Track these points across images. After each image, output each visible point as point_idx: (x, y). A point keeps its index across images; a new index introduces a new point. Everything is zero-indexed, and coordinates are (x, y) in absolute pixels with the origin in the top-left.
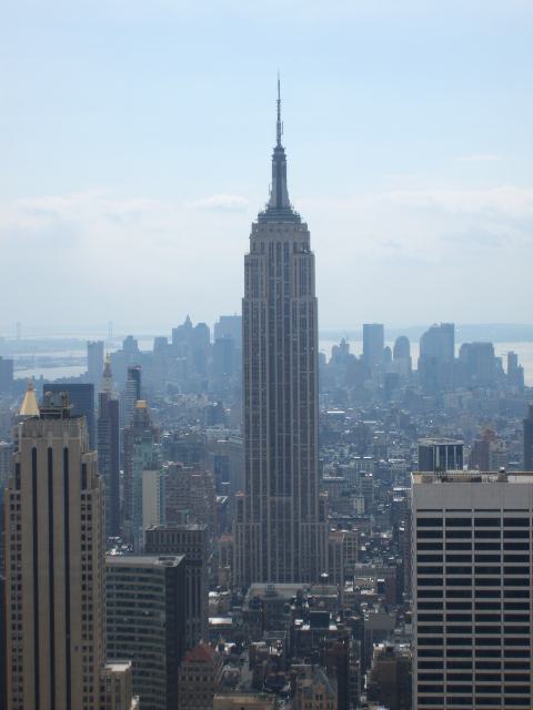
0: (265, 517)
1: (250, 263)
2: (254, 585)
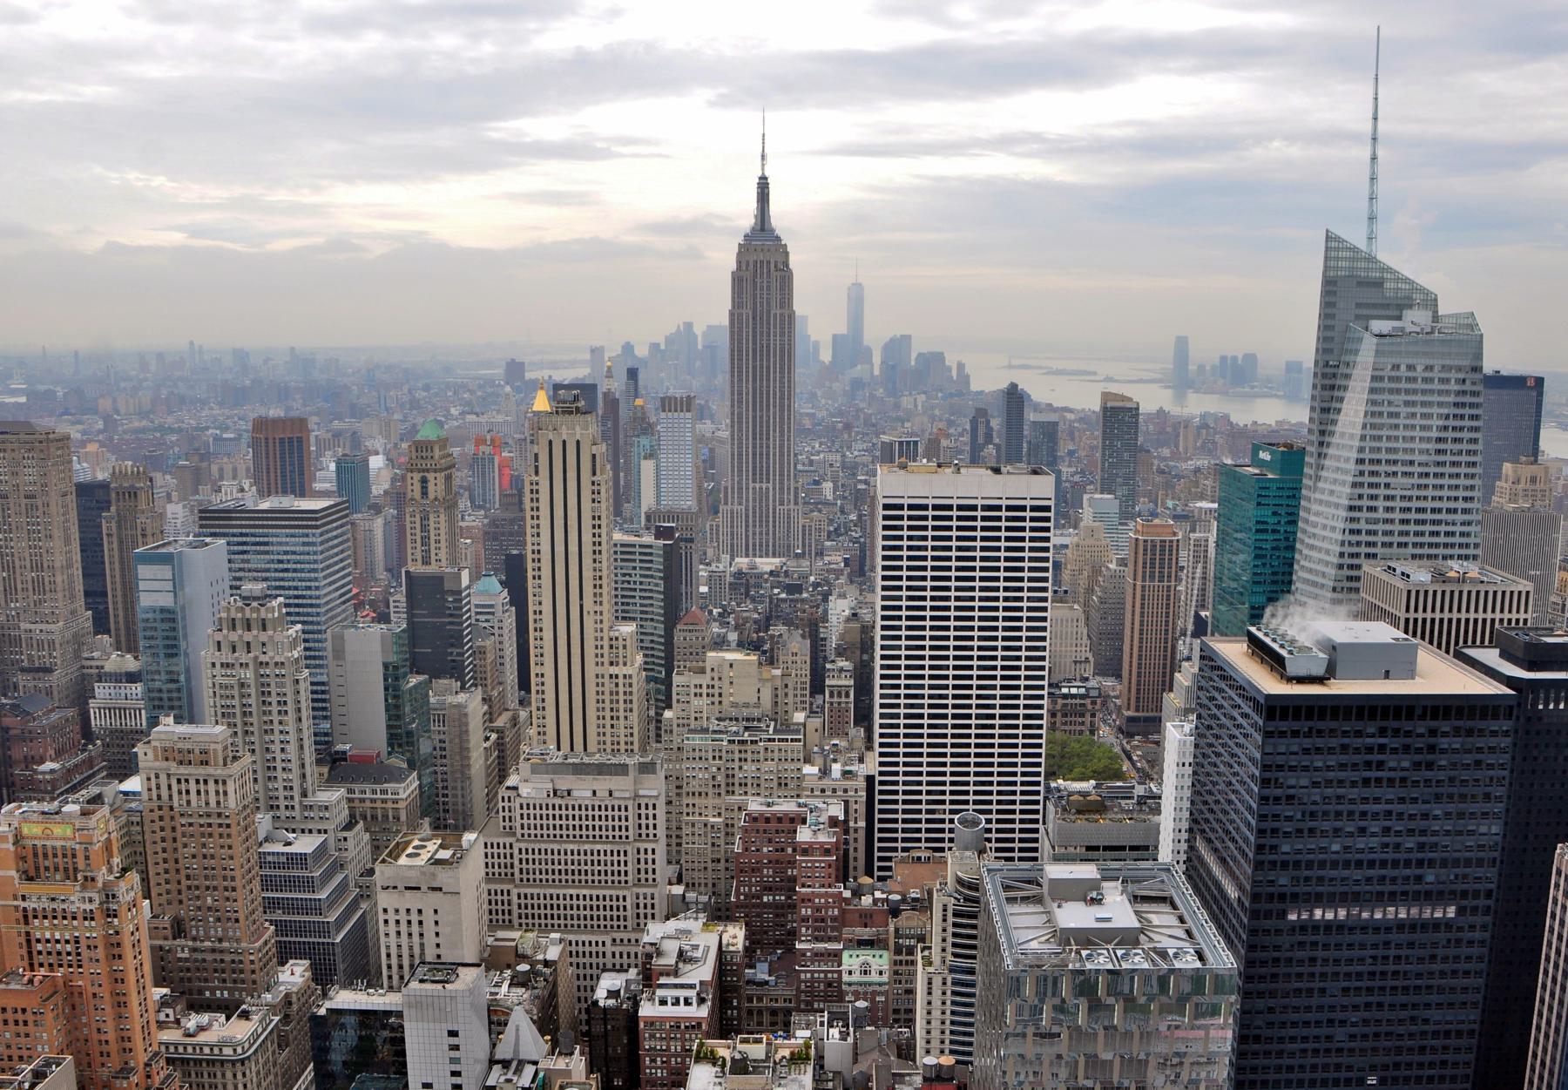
0: (747, 500)
1: (738, 280)
2: (738, 560)
